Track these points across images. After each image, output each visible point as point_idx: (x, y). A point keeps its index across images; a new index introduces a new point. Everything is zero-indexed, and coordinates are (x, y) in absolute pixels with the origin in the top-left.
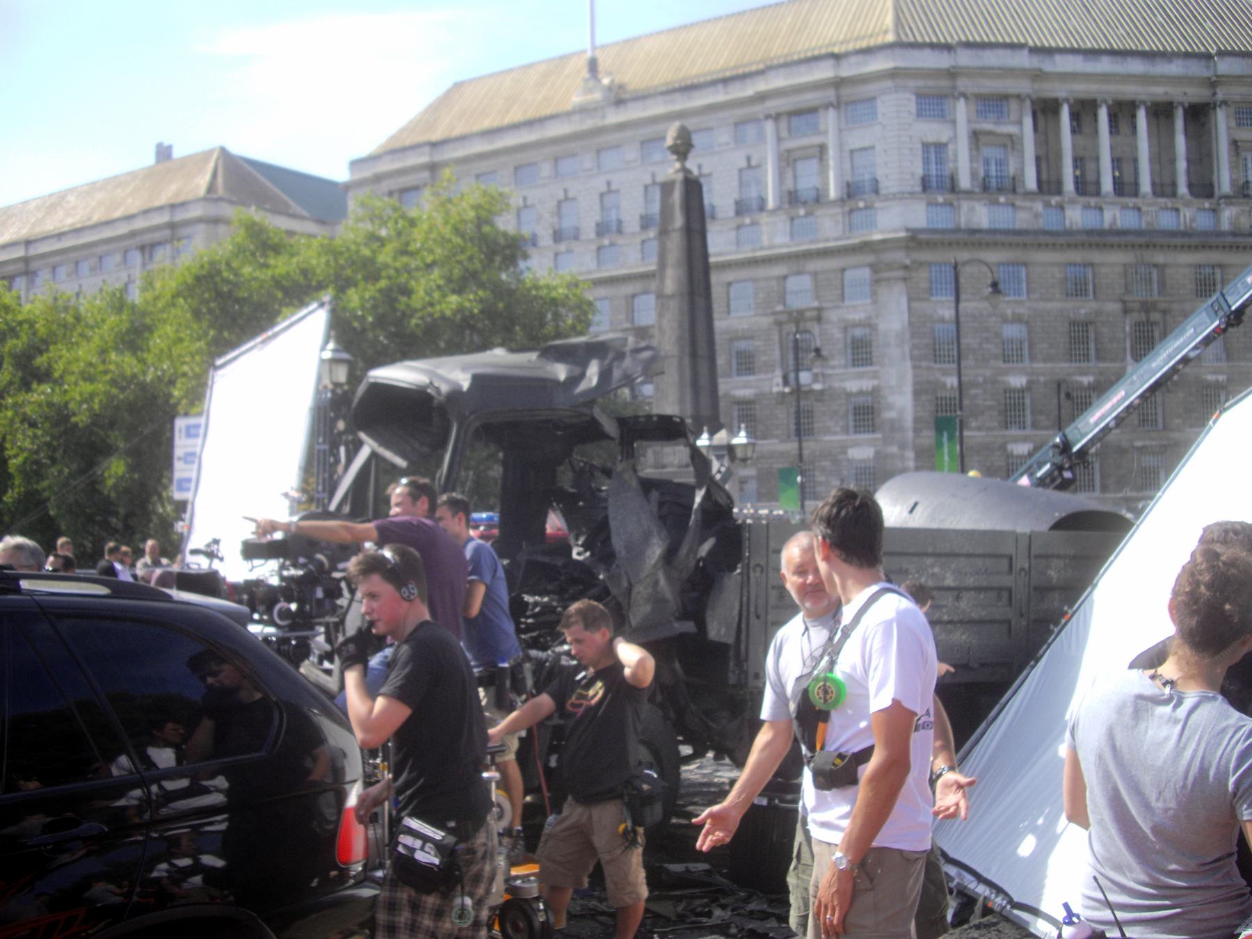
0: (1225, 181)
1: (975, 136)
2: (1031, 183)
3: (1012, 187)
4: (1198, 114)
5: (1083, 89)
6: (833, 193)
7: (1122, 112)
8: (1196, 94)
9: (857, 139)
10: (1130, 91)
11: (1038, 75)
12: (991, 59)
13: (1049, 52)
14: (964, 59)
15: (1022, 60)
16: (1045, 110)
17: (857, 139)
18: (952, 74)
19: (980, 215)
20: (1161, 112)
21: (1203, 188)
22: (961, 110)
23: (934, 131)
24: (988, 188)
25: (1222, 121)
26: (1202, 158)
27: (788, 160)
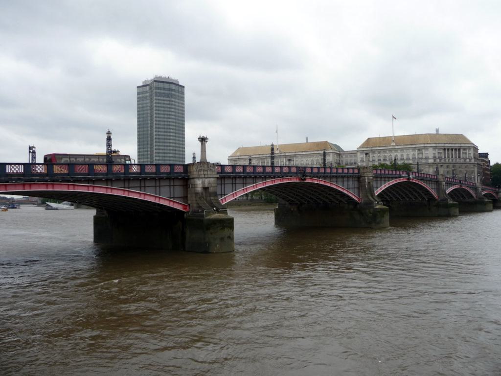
0: (462, 157)
1: (438, 152)
3: (441, 158)
4: (459, 150)
6: (424, 157)
9: (427, 152)
10: (452, 148)
11: (444, 146)
12: (440, 145)
13: (445, 144)
14: (437, 145)
15: (443, 145)
16: (445, 149)
17: (427, 152)
18: (436, 146)
20: (456, 149)
21: (459, 157)
22: (437, 150)
23: (435, 152)
25: (462, 151)
26: (459, 154)
27: (418, 154)
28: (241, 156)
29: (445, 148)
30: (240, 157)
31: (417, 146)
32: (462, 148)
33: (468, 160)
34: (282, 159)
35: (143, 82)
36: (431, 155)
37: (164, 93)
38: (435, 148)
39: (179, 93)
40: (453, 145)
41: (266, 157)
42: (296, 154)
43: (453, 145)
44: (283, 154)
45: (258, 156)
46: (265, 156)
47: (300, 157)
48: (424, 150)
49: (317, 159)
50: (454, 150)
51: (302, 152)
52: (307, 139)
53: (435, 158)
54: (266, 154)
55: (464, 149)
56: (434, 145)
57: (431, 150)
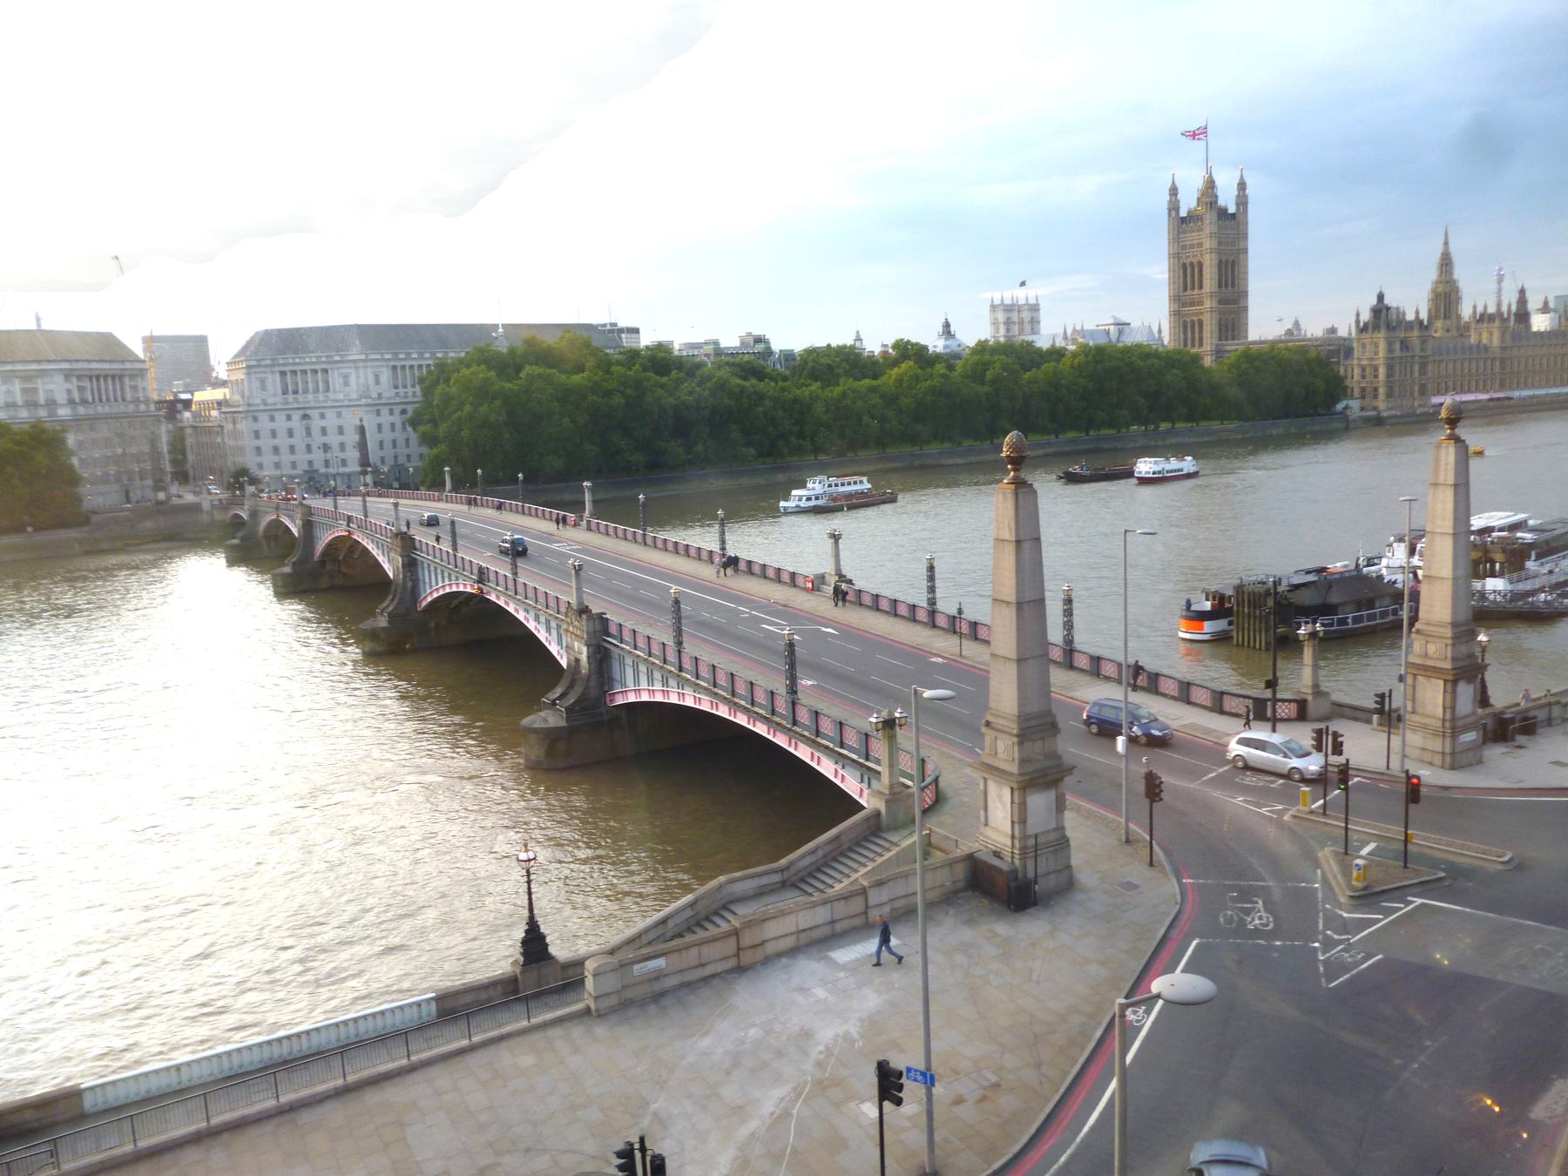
0: (129, 396)
2: (90, 399)
4: (121, 377)
5: (98, 372)
6: (42, 402)
7: (106, 377)
8: (119, 373)
10: (107, 372)
15: (86, 365)
18: (72, 370)
19: (81, 410)
20: (113, 377)
22: (74, 380)
23: (69, 386)
24: (84, 402)
25: (127, 381)
26: (122, 390)
27: (24, 391)
29: (93, 373)
31: (19, 367)
32: (126, 373)
33: (142, 407)
36: (61, 397)
38: (68, 375)
40: (107, 366)
43: (107, 366)
48: (39, 380)
50: (102, 379)
53: (71, 402)
55: (132, 377)
56: (66, 366)
57: (59, 379)
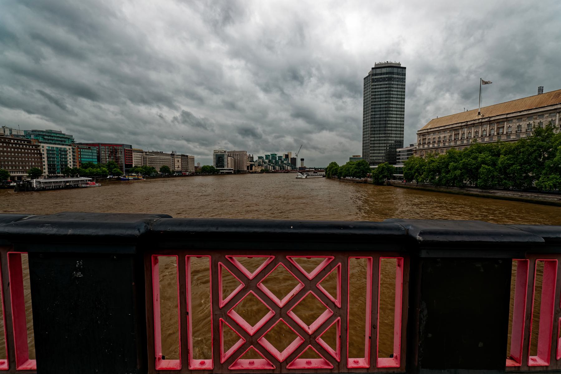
28: (430, 129)
30: (429, 131)
34: (485, 126)
35: (369, 73)
37: (381, 78)
39: (398, 75)
41: (461, 126)
42: (508, 116)
44: (487, 120)
45: (451, 126)
46: (460, 125)
47: (514, 121)
49: (550, 119)
51: (520, 112)
52: (541, 90)
54: (462, 123)
